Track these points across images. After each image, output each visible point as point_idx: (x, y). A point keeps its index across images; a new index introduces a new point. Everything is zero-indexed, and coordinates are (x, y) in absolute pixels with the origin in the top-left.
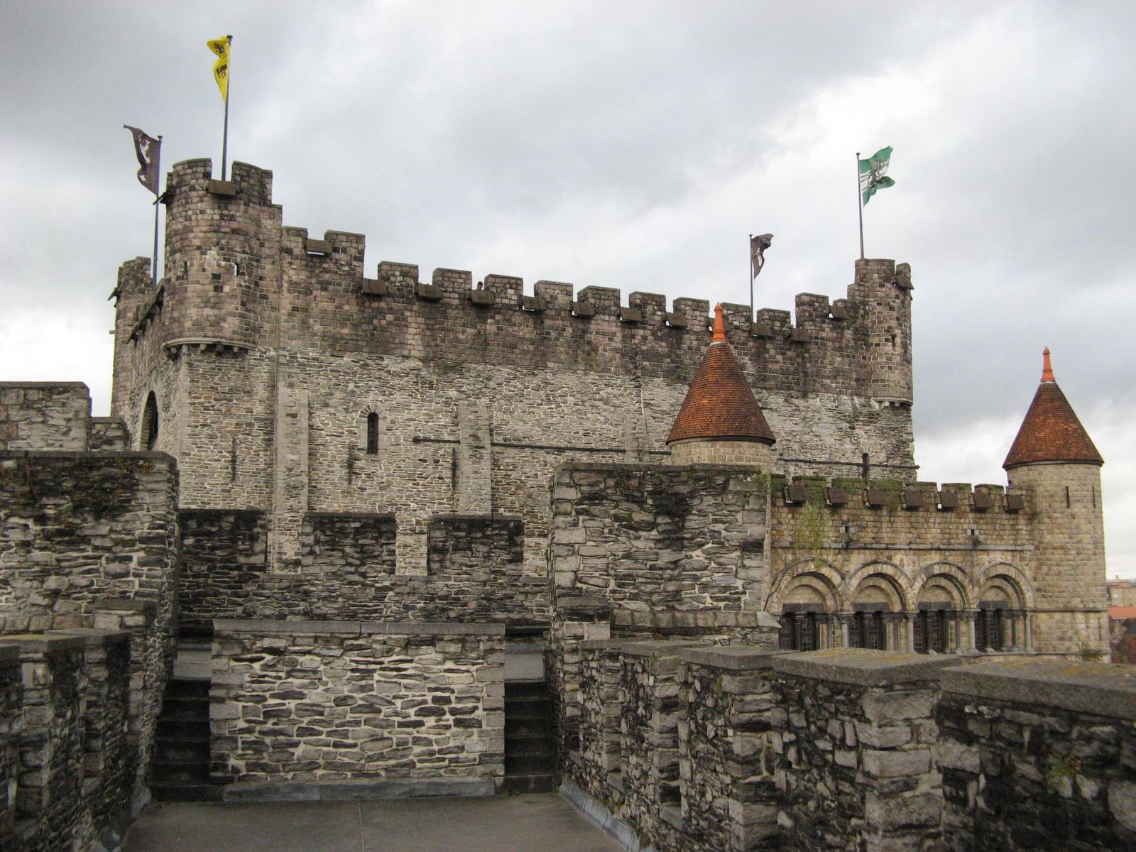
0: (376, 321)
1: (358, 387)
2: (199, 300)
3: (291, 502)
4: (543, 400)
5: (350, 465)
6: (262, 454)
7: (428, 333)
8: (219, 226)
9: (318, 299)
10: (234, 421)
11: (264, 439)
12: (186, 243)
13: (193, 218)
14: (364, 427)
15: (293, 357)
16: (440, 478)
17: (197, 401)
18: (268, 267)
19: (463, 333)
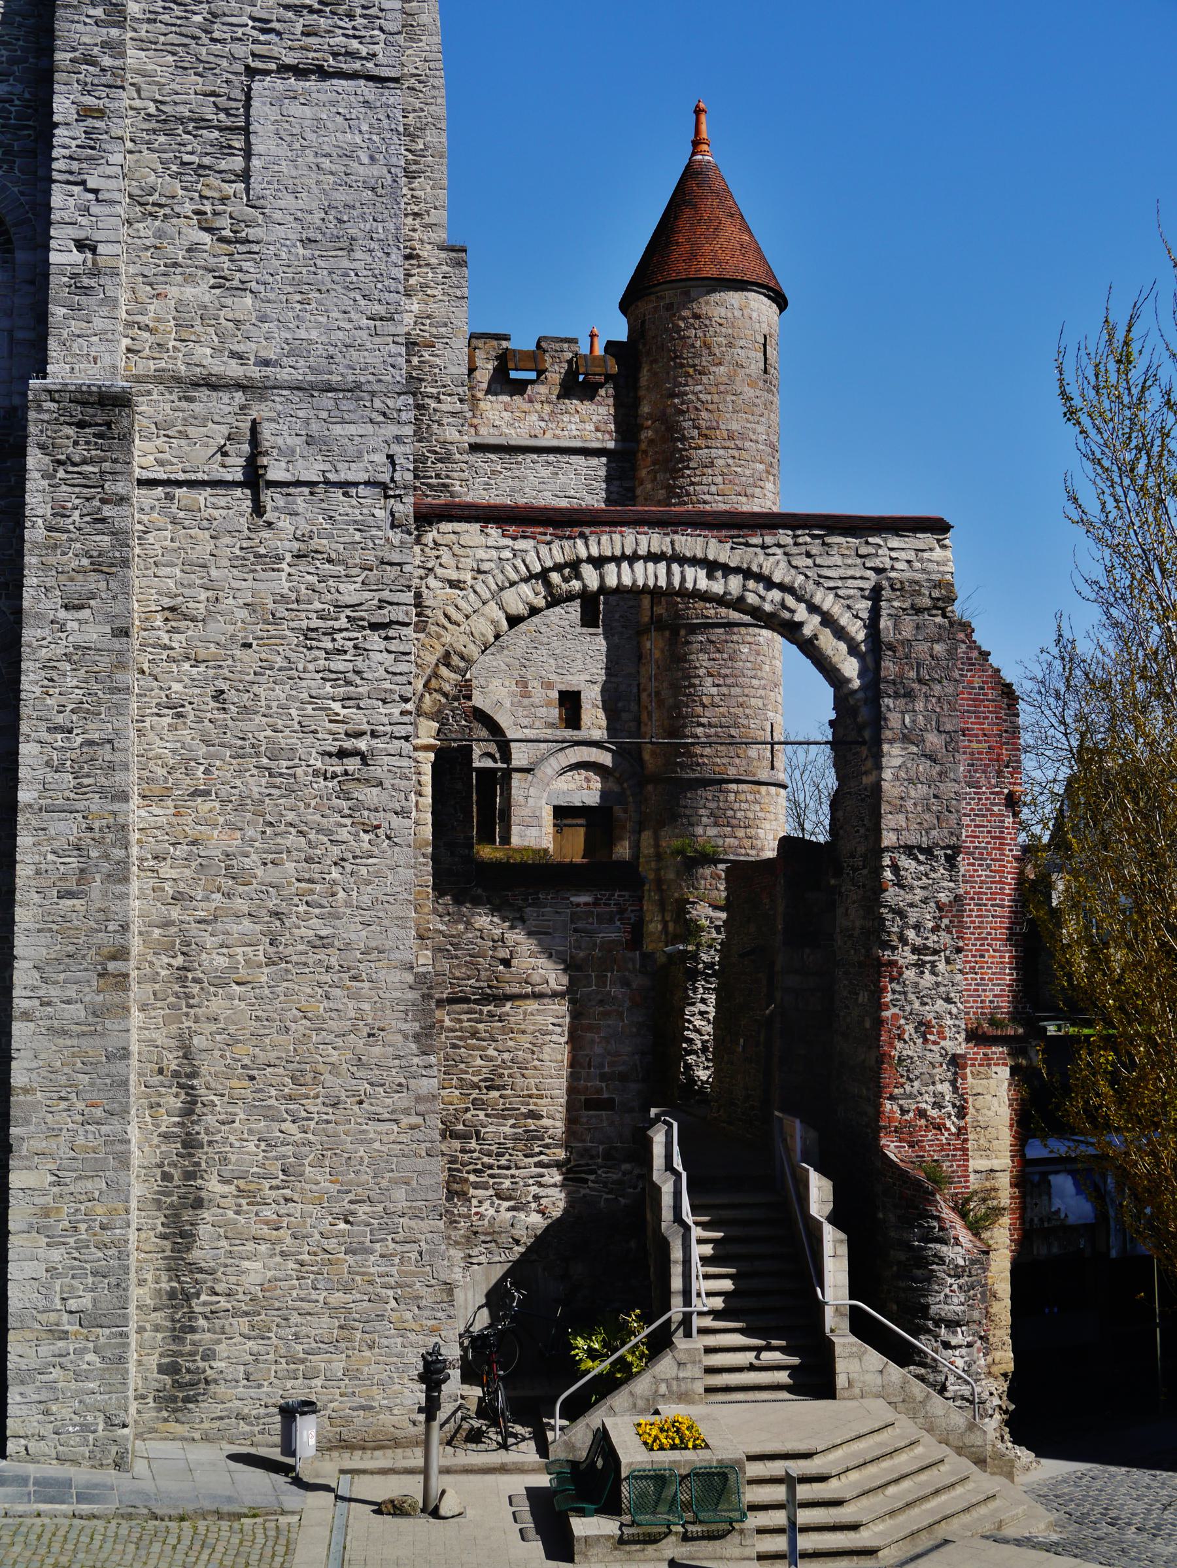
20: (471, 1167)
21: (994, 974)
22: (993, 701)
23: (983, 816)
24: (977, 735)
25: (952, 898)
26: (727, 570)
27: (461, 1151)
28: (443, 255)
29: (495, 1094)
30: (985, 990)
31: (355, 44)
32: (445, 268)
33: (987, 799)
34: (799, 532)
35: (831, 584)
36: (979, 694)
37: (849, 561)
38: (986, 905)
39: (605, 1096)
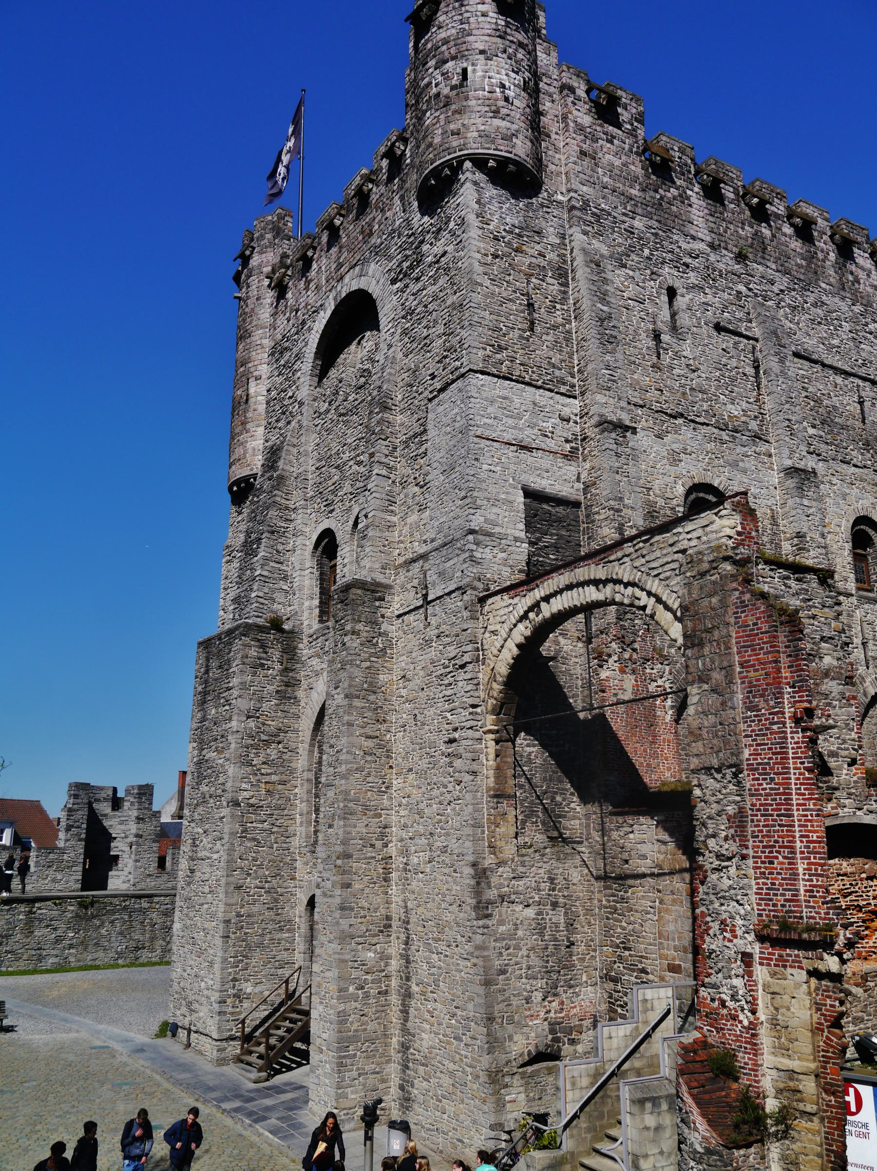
0: (660, 191)
1: (653, 255)
2: (487, 109)
3: (608, 357)
4: (822, 319)
5: (657, 337)
6: (558, 306)
7: (711, 219)
8: (505, 33)
9: (605, 150)
10: (527, 261)
11: (560, 291)
12: (464, 47)
13: (472, 20)
14: (665, 298)
15: (586, 203)
16: (745, 375)
17: (485, 226)
18: (548, 104)
19: (743, 229)
20: (619, 1003)
21: (783, 879)
22: (766, 632)
23: (763, 735)
24: (753, 666)
25: (737, 811)
26: (605, 582)
27: (615, 991)
28: (597, 430)
29: (627, 953)
30: (776, 895)
31: (457, 363)
32: (598, 437)
33: (766, 720)
34: (635, 542)
35: (656, 572)
36: (753, 630)
37: (665, 552)
38: (772, 815)
39: (677, 963)
